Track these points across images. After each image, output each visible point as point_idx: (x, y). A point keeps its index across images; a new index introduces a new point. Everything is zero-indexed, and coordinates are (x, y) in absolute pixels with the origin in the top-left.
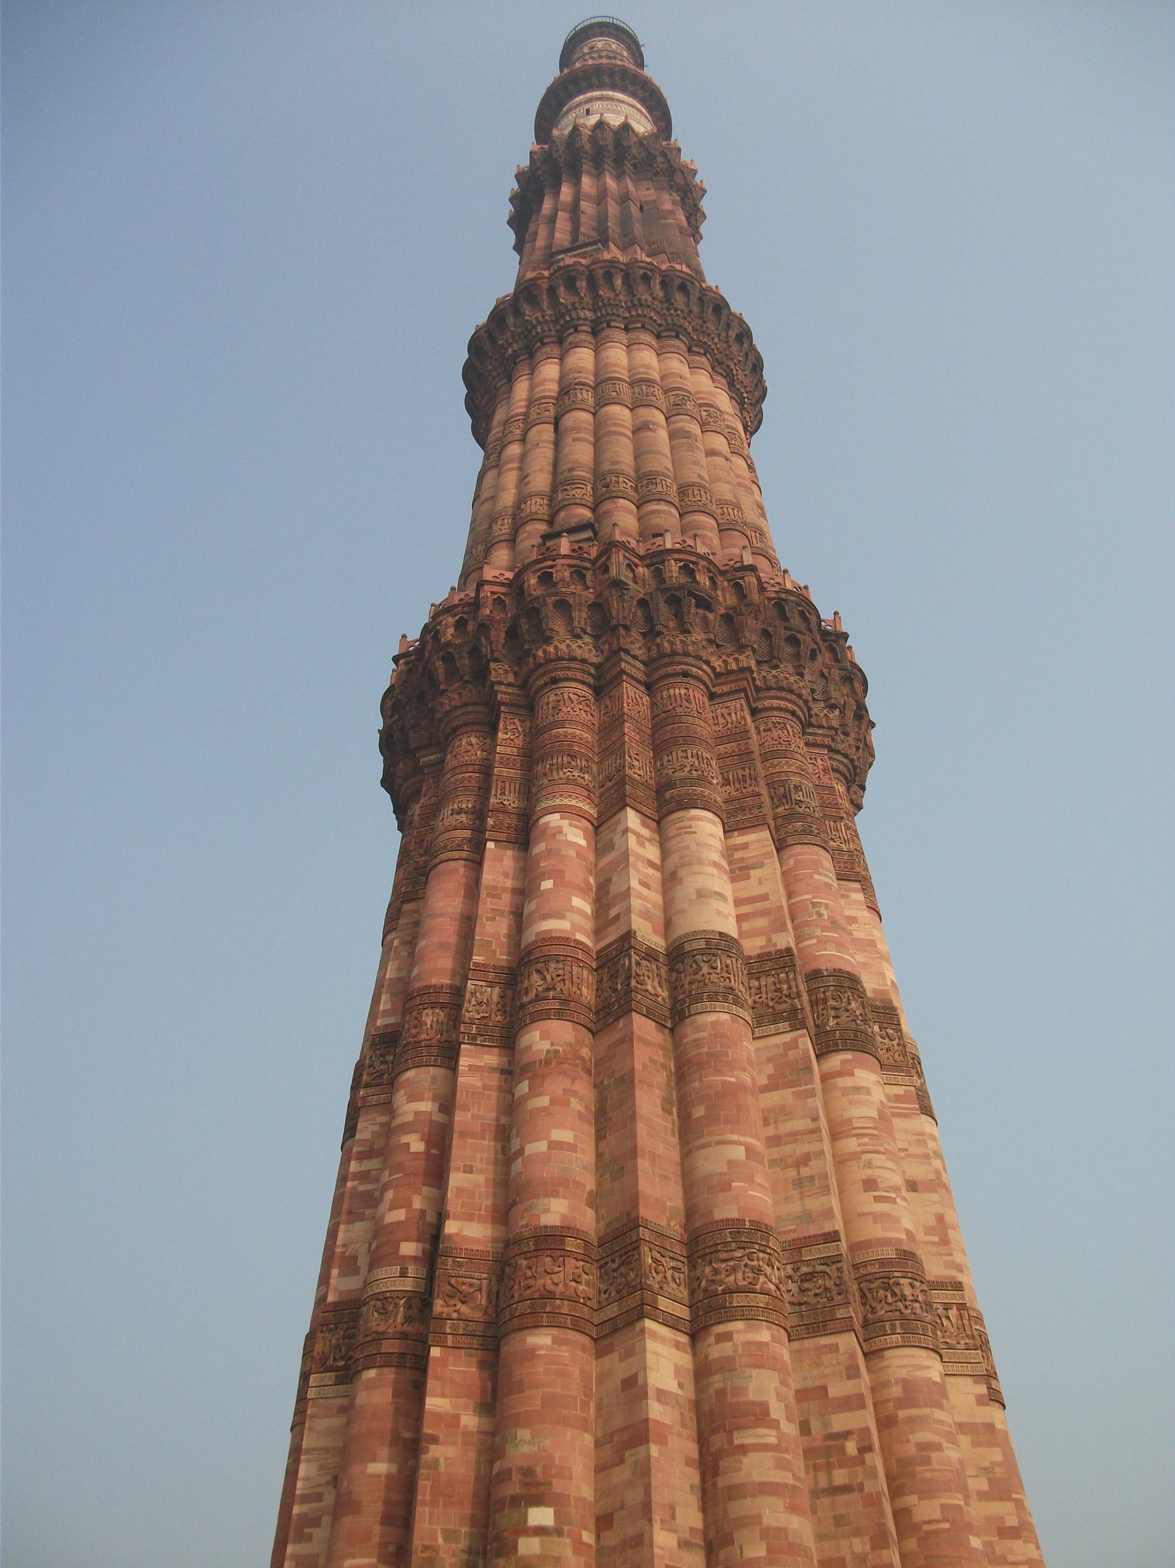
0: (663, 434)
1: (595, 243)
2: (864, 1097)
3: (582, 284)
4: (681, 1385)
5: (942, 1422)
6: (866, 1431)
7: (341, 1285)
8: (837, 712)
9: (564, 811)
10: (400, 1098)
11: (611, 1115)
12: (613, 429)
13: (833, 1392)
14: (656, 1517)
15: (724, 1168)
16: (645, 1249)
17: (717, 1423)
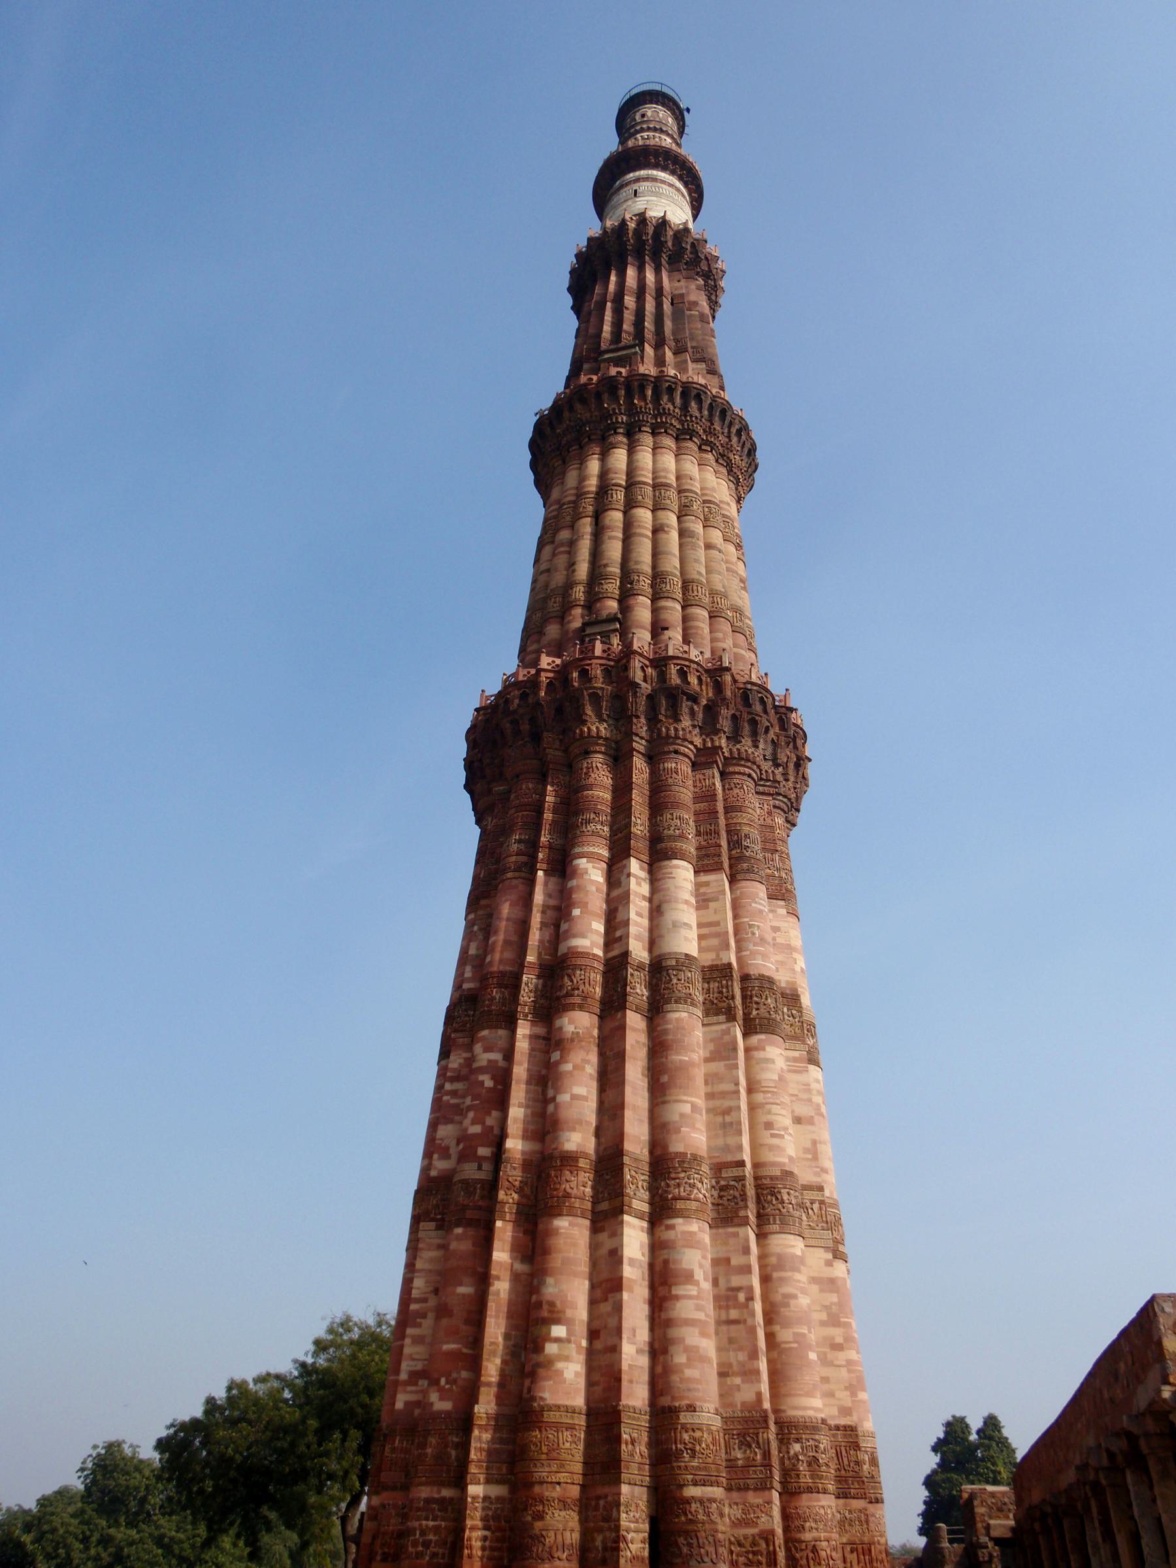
0: (674, 535)
1: (633, 346)
2: (772, 1066)
4: (643, 1255)
5: (799, 1281)
6: (750, 1289)
7: (440, 1165)
8: (781, 769)
9: (590, 856)
10: (478, 1048)
12: (638, 531)
13: (734, 1262)
14: (624, 1336)
15: (676, 1118)
16: (626, 1170)
17: (663, 1279)
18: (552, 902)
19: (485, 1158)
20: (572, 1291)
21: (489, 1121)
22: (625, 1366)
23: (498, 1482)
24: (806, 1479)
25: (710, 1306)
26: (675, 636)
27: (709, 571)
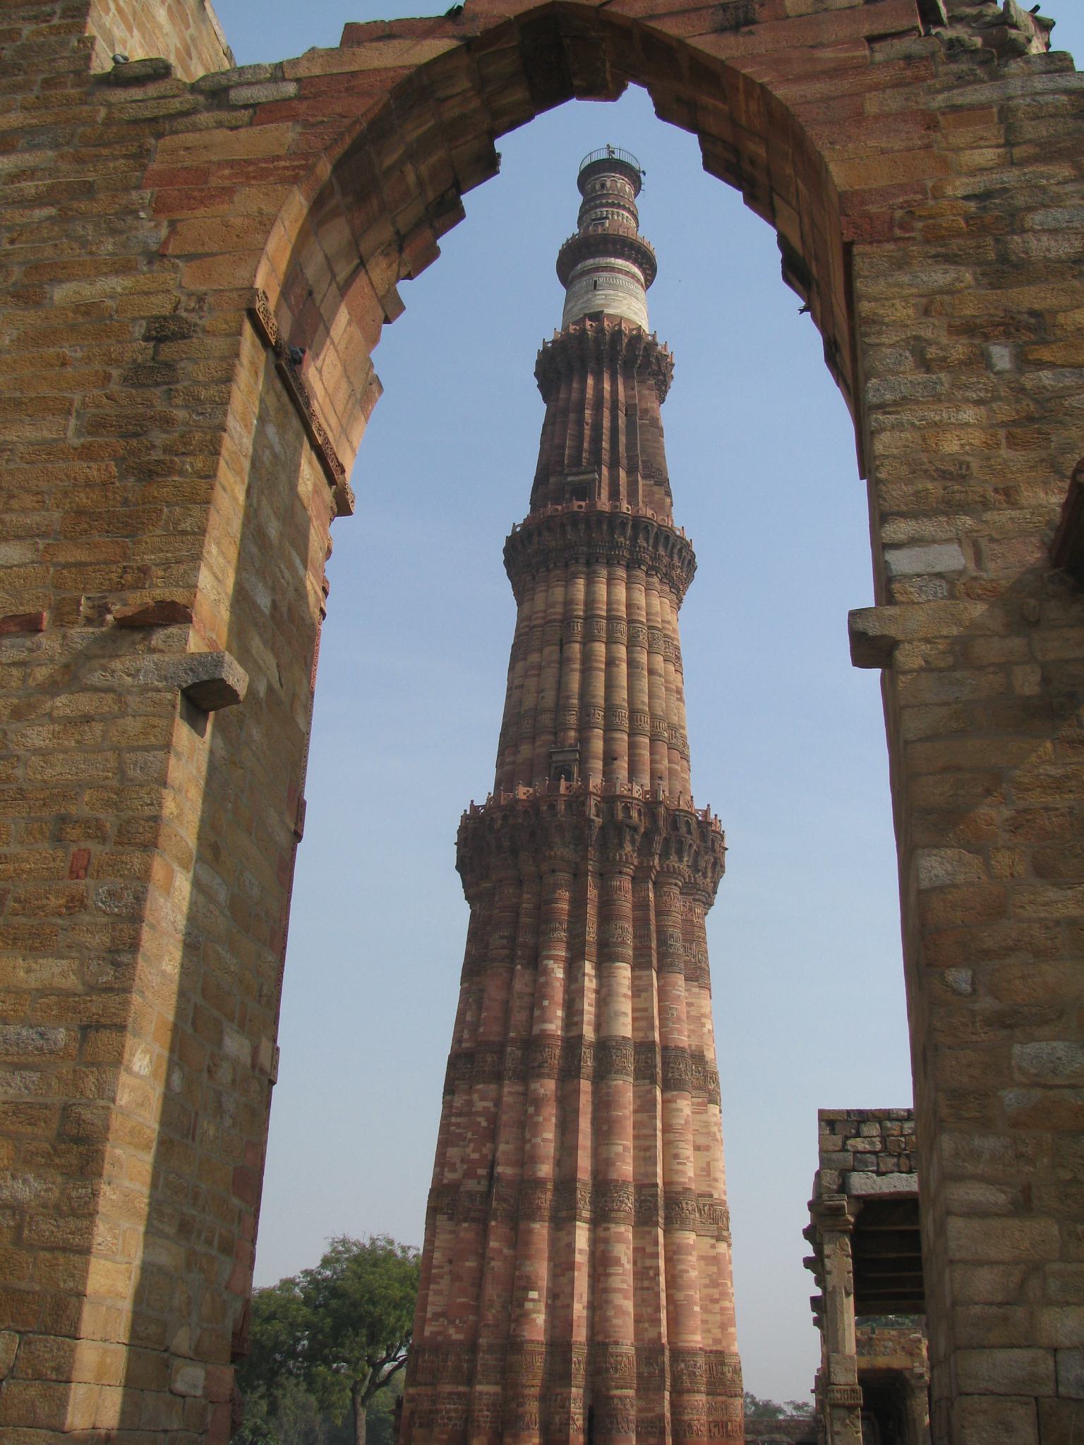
0: (624, 666)
1: (593, 472)
3: (582, 527)
6: (658, 1268)
7: (449, 1176)
9: (556, 959)
10: (475, 1097)
11: (567, 1126)
12: (596, 665)
18: (528, 990)
19: (483, 1176)
20: (541, 1269)
21: (485, 1151)
22: (575, 1317)
23: (496, 1384)
24: (687, 1384)
25: (630, 1280)
26: (623, 765)
27: (651, 696)
